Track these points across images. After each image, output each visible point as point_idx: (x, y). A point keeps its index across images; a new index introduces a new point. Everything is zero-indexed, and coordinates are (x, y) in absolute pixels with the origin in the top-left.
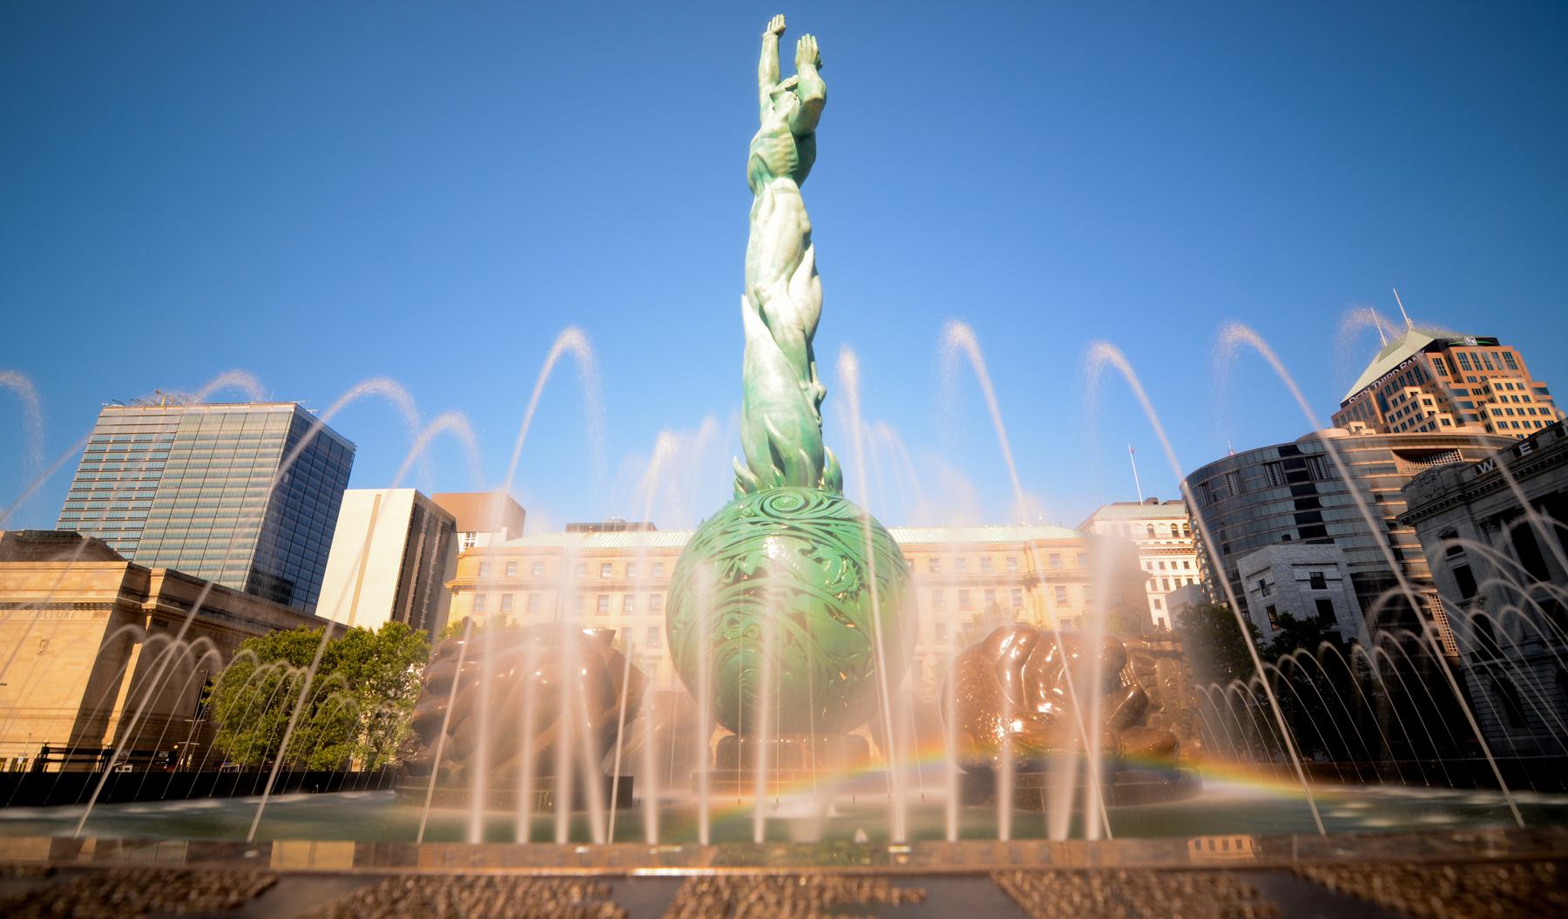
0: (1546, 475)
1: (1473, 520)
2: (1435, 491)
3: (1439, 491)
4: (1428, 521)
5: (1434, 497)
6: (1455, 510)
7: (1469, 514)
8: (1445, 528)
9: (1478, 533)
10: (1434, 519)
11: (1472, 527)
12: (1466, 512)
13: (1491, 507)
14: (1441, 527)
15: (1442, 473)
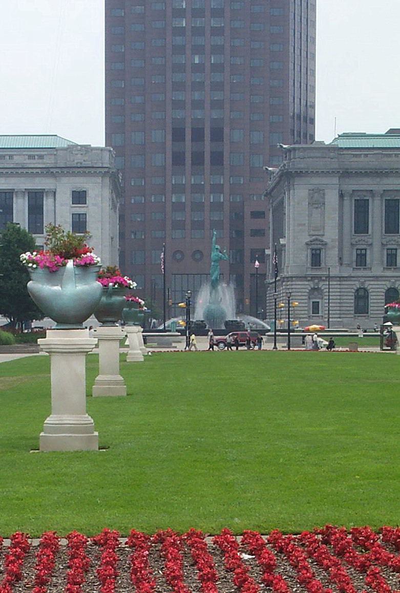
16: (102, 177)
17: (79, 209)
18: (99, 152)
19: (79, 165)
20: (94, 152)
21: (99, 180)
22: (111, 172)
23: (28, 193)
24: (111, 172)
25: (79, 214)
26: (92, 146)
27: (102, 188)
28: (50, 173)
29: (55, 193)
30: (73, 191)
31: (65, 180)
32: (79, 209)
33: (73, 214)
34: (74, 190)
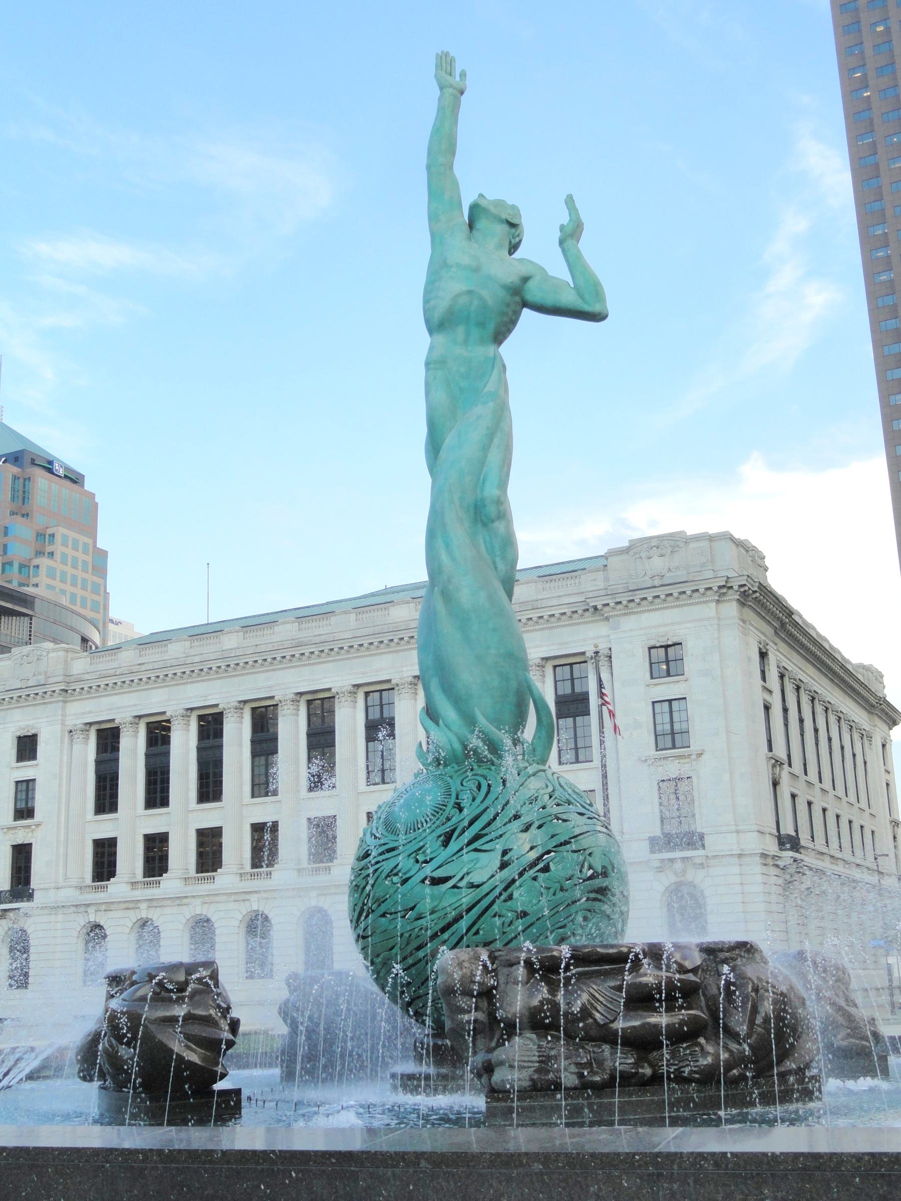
0: (161, 690)
1: (63, 724)
2: (34, 675)
3: (40, 677)
4: (9, 712)
5: (30, 683)
6: (49, 706)
7: (62, 715)
8: (28, 726)
9: (62, 742)
10: (17, 710)
11: (59, 734)
12: (60, 712)
13: (90, 712)
14: (22, 724)
15: (51, 655)
16: (718, 601)
17: (667, 689)
18: (705, 544)
19: (657, 582)
20: (692, 545)
21: (710, 610)
22: (736, 588)
23: (555, 667)
24: (736, 588)
25: (670, 701)
26: (690, 532)
27: (719, 630)
28: (591, 610)
29: (610, 657)
30: (650, 648)
31: (629, 623)
32: (667, 689)
33: (654, 703)
34: (652, 643)
